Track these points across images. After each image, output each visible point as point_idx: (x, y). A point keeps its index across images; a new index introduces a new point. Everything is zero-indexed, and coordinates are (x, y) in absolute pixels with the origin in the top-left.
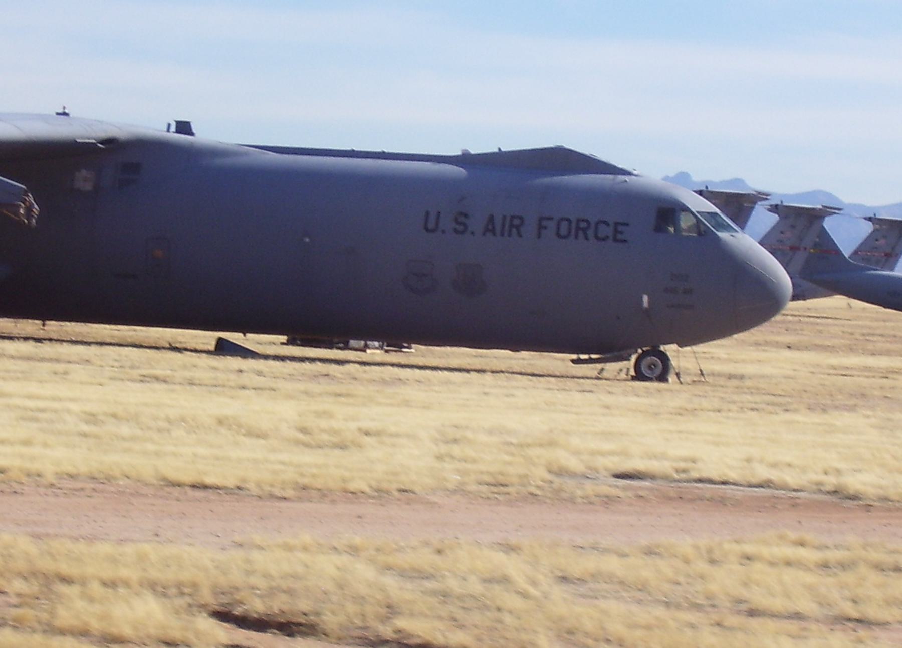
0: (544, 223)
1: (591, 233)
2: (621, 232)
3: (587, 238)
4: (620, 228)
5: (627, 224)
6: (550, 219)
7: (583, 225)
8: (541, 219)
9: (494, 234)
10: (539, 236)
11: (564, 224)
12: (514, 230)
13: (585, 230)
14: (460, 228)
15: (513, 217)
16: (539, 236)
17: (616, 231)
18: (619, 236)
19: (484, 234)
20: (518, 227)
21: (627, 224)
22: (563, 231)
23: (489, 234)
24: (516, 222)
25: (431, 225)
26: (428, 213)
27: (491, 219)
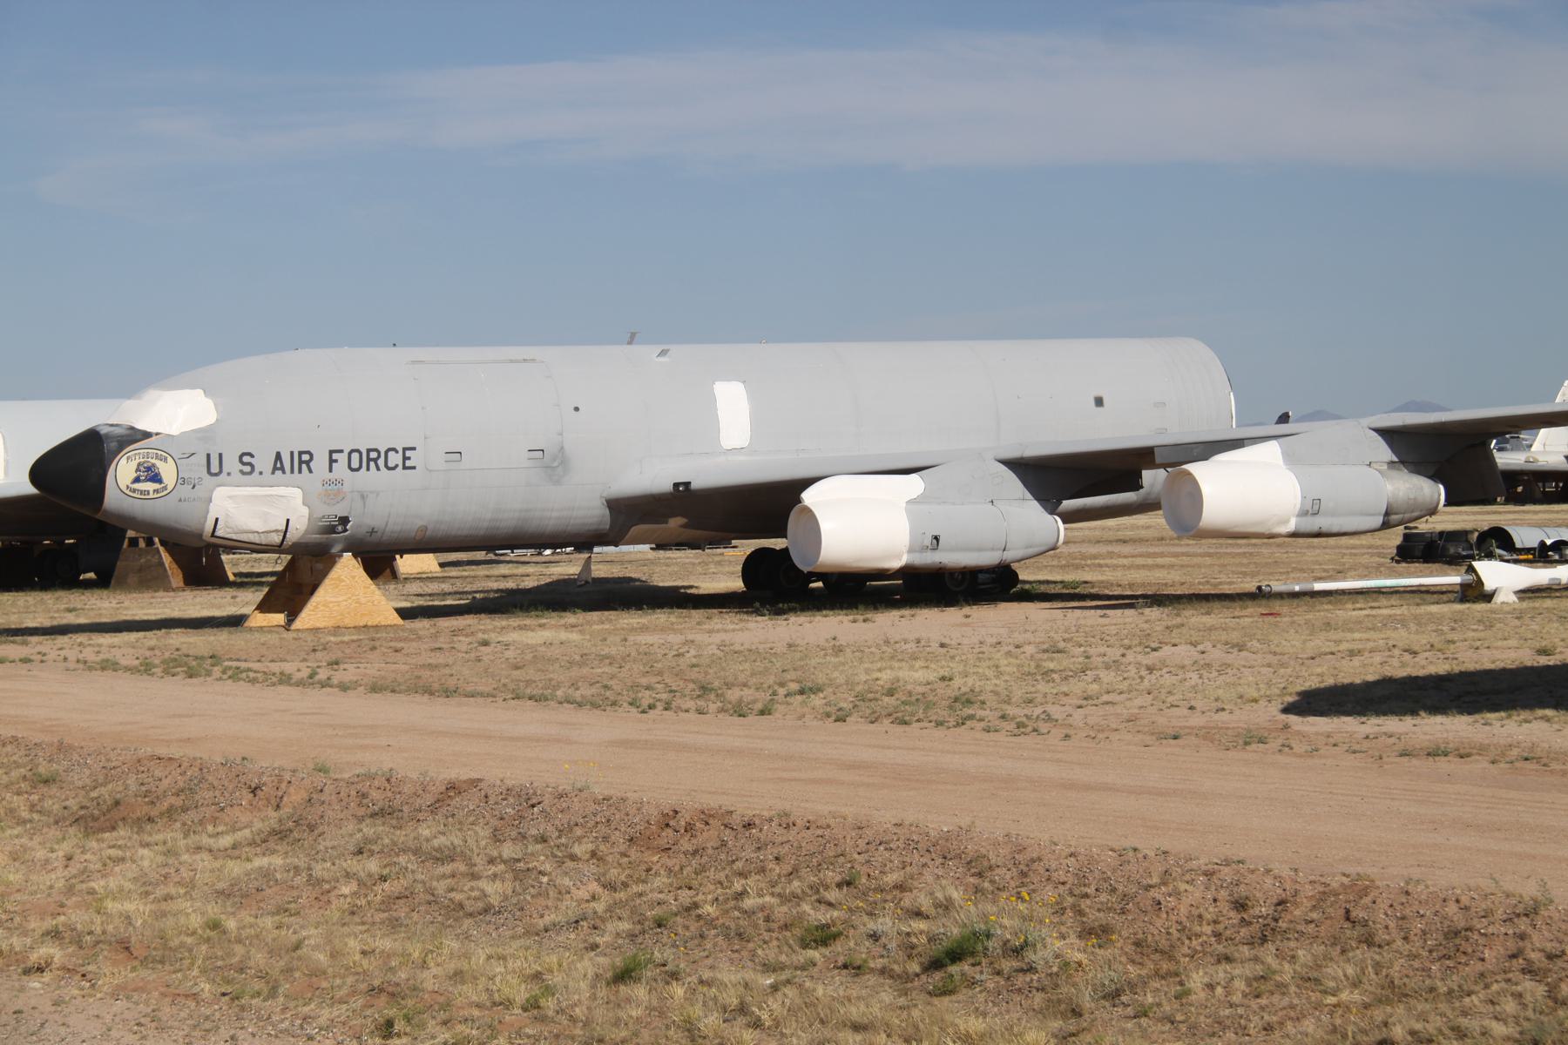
0: (335, 456)
1: (381, 462)
2: (409, 458)
3: (378, 469)
4: (408, 453)
5: (414, 449)
6: (341, 451)
7: (373, 455)
8: (331, 452)
9: (284, 472)
10: (331, 471)
11: (355, 456)
12: (304, 466)
13: (375, 460)
14: (247, 469)
15: (300, 453)
16: (331, 471)
17: (405, 458)
18: (408, 463)
19: (273, 473)
20: (308, 463)
21: (414, 449)
22: (355, 464)
23: (279, 473)
24: (305, 457)
25: (215, 469)
26: (208, 456)
27: (278, 456)
